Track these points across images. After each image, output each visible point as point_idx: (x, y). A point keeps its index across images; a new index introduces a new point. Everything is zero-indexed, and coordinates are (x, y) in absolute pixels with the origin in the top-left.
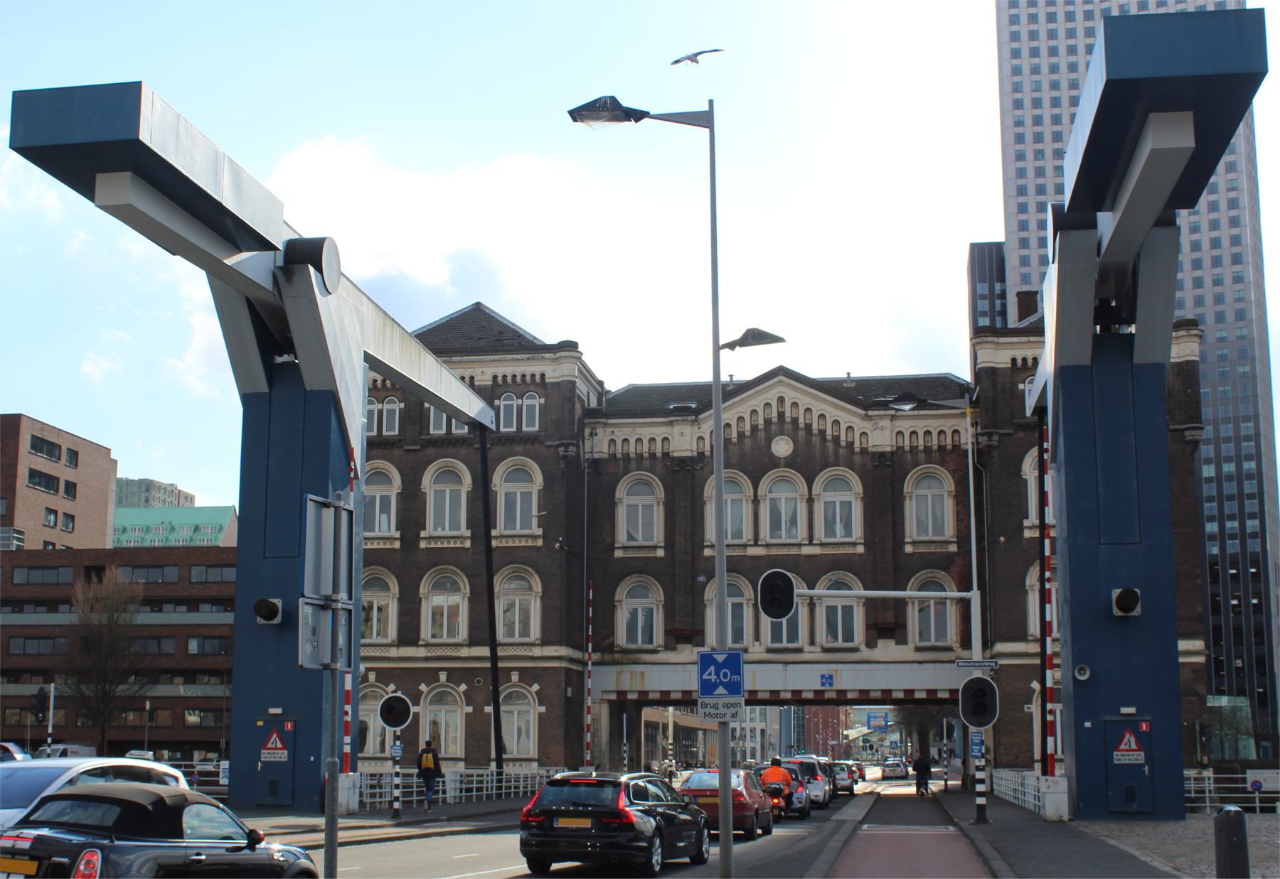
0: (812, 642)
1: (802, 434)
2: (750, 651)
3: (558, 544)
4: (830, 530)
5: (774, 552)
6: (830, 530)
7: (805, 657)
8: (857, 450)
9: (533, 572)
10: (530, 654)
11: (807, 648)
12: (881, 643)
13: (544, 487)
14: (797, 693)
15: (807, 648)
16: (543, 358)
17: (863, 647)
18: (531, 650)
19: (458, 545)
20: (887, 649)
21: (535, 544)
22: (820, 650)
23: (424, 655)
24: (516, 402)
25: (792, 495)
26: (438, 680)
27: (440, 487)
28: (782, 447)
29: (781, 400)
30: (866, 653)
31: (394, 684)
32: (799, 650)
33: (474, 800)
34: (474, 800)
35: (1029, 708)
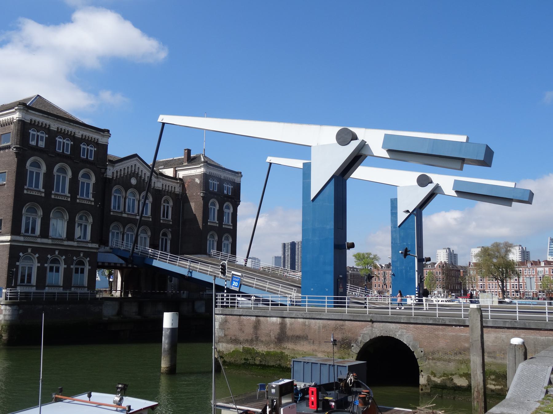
1: (139, 178)
5: (130, 216)
9: (90, 215)
10: (87, 246)
14: (109, 263)
16: (100, 133)
19: (65, 199)
23: (23, 240)
25: (134, 198)
26: (55, 254)
27: (59, 174)
28: (134, 181)
29: (135, 165)
33: (230, 307)
34: (230, 307)
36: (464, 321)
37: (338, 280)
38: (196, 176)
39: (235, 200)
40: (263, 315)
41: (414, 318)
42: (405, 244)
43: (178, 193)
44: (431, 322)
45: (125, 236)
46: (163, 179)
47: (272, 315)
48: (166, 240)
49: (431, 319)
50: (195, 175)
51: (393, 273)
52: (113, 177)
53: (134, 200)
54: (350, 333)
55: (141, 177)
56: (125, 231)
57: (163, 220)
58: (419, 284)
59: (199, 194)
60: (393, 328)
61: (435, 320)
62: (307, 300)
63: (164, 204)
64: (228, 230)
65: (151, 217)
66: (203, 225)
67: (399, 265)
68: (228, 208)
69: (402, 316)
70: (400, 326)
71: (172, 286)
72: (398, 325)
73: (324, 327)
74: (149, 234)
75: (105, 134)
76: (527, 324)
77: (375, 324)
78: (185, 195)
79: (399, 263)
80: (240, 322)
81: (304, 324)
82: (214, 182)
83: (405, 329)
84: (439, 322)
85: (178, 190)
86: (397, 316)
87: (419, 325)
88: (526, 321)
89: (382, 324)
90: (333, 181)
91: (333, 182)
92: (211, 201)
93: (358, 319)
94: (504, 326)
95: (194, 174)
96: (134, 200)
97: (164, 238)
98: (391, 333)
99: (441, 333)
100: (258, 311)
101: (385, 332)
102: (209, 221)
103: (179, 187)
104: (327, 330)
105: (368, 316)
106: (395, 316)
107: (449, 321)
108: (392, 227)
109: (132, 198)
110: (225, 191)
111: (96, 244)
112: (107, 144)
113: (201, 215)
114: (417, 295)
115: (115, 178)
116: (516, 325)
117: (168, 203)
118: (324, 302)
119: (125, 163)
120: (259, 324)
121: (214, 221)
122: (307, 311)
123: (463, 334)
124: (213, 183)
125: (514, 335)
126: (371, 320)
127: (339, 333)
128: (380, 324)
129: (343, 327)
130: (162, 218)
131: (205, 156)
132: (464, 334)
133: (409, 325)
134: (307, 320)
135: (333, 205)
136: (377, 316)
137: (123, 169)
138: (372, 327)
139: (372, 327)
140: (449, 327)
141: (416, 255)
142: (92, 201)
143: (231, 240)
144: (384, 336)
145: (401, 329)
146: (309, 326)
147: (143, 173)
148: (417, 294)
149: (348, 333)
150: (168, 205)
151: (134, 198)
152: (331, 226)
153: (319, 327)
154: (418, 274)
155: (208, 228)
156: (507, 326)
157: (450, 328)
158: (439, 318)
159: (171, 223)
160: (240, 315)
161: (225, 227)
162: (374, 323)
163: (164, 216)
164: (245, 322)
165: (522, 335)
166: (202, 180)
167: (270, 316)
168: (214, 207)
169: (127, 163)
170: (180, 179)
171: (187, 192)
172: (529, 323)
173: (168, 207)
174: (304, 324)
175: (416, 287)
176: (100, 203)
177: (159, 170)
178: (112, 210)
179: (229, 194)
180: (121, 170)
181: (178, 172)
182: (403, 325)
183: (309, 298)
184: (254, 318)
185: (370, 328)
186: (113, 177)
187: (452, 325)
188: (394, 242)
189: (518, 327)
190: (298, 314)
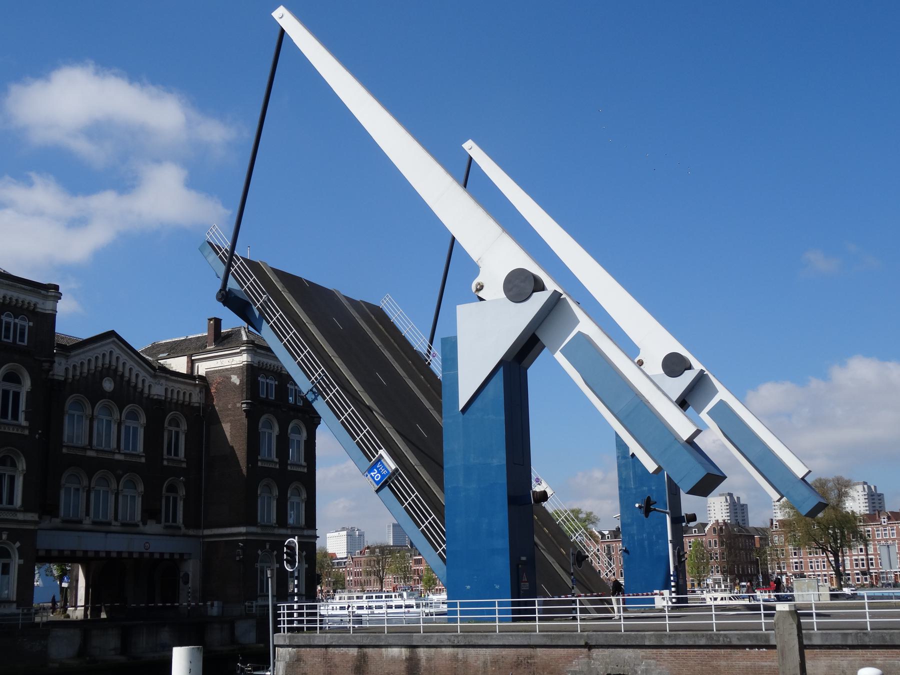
0: (116, 519)
2: (84, 522)
3: (37, 436)
4: (127, 447)
5: (101, 455)
6: (127, 447)
7: (113, 528)
8: (145, 395)
9: (22, 455)
11: (114, 523)
12: (149, 522)
13: (31, 390)
14: (61, 551)
15: (114, 523)
16: (40, 293)
17: (141, 524)
18: (16, 515)
20: (152, 527)
21: (22, 433)
22: (119, 524)
24: (11, 320)
25: (109, 418)
28: (108, 385)
29: (111, 352)
30: (142, 528)
31: (19, 542)
32: (109, 524)
33: (305, 630)
34: (305, 630)
35: (257, 565)
36: (767, 637)
37: (518, 566)
38: (232, 370)
39: (310, 415)
40: (373, 644)
41: (670, 636)
42: (645, 488)
43: (197, 405)
44: (703, 642)
45: (92, 496)
46: (167, 377)
47: (391, 642)
48: (175, 500)
49: (703, 636)
50: (231, 368)
51: (624, 548)
52: (66, 379)
53: (109, 423)
54: (546, 673)
55: (122, 376)
56: (92, 485)
57: (168, 460)
58: (676, 568)
59: (238, 405)
60: (630, 657)
61: (710, 637)
62: (458, 608)
63: (170, 428)
64: (297, 476)
65: (144, 454)
66: (248, 468)
67: (635, 532)
68: (297, 431)
69: (646, 633)
70: (643, 653)
71: (189, 592)
72: (638, 651)
73: (495, 662)
74: (141, 488)
75: (50, 294)
76: (888, 638)
77: (595, 652)
78: (210, 408)
79: (635, 527)
80: (327, 660)
81: (455, 658)
82: (268, 381)
83: (654, 659)
84: (719, 641)
85: (197, 398)
86: (636, 633)
87: (680, 650)
88: (885, 631)
89: (607, 652)
90: (502, 369)
91: (500, 373)
92: (263, 418)
93: (560, 643)
94: (844, 643)
95: (229, 367)
96: (109, 423)
97: (171, 496)
98: (627, 668)
99: (723, 663)
100: (363, 636)
101: (615, 667)
102: (259, 458)
103: (199, 394)
104: (500, 668)
105: (581, 637)
106: (633, 633)
107: (738, 639)
108: (618, 457)
109: (105, 418)
110: (291, 398)
111: (33, 514)
112: (54, 313)
113: (245, 447)
114: (673, 589)
115: (70, 380)
116: (867, 641)
117: (178, 426)
118: (493, 612)
119: (90, 350)
120: (365, 661)
121: (269, 459)
122: (460, 632)
123: (765, 664)
124: (267, 383)
125: (864, 660)
126: (586, 643)
127: (524, 672)
128: (604, 651)
129: (533, 661)
130: (165, 457)
131: (249, 331)
132: (769, 663)
133: (661, 650)
134: (460, 650)
135: (503, 418)
136: (598, 635)
137: (86, 362)
138: (589, 657)
139: (589, 657)
140: (738, 650)
141: (668, 511)
142: (23, 428)
143: (304, 496)
144: (612, 674)
145: (646, 659)
146: (465, 661)
147: (128, 367)
148: (673, 586)
149: (542, 673)
150: (176, 429)
151: (109, 418)
152: (499, 459)
153: (485, 663)
154: (674, 548)
155: (257, 473)
156: (850, 642)
157: (739, 653)
158: (718, 632)
159: (184, 465)
160: (327, 646)
161: (292, 469)
162: (593, 650)
163: (169, 452)
164: (337, 660)
165: (879, 659)
166: (245, 378)
167: (387, 644)
168: (270, 431)
169: (94, 349)
170: (200, 377)
171: (214, 403)
172: (891, 635)
173: (177, 434)
174: (455, 658)
175: (672, 573)
176: (40, 432)
177: (159, 361)
178: (64, 444)
179: (298, 404)
180: (82, 363)
181: (197, 364)
182: (648, 651)
183: (462, 605)
184: (354, 651)
185: (586, 660)
186: (66, 379)
187: (744, 647)
188: (623, 486)
189: (871, 644)
190: (443, 639)
